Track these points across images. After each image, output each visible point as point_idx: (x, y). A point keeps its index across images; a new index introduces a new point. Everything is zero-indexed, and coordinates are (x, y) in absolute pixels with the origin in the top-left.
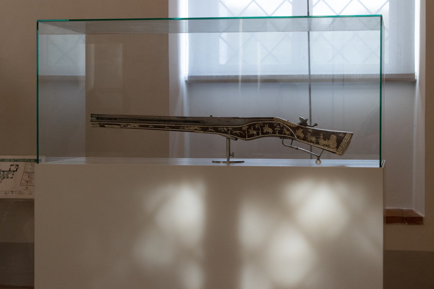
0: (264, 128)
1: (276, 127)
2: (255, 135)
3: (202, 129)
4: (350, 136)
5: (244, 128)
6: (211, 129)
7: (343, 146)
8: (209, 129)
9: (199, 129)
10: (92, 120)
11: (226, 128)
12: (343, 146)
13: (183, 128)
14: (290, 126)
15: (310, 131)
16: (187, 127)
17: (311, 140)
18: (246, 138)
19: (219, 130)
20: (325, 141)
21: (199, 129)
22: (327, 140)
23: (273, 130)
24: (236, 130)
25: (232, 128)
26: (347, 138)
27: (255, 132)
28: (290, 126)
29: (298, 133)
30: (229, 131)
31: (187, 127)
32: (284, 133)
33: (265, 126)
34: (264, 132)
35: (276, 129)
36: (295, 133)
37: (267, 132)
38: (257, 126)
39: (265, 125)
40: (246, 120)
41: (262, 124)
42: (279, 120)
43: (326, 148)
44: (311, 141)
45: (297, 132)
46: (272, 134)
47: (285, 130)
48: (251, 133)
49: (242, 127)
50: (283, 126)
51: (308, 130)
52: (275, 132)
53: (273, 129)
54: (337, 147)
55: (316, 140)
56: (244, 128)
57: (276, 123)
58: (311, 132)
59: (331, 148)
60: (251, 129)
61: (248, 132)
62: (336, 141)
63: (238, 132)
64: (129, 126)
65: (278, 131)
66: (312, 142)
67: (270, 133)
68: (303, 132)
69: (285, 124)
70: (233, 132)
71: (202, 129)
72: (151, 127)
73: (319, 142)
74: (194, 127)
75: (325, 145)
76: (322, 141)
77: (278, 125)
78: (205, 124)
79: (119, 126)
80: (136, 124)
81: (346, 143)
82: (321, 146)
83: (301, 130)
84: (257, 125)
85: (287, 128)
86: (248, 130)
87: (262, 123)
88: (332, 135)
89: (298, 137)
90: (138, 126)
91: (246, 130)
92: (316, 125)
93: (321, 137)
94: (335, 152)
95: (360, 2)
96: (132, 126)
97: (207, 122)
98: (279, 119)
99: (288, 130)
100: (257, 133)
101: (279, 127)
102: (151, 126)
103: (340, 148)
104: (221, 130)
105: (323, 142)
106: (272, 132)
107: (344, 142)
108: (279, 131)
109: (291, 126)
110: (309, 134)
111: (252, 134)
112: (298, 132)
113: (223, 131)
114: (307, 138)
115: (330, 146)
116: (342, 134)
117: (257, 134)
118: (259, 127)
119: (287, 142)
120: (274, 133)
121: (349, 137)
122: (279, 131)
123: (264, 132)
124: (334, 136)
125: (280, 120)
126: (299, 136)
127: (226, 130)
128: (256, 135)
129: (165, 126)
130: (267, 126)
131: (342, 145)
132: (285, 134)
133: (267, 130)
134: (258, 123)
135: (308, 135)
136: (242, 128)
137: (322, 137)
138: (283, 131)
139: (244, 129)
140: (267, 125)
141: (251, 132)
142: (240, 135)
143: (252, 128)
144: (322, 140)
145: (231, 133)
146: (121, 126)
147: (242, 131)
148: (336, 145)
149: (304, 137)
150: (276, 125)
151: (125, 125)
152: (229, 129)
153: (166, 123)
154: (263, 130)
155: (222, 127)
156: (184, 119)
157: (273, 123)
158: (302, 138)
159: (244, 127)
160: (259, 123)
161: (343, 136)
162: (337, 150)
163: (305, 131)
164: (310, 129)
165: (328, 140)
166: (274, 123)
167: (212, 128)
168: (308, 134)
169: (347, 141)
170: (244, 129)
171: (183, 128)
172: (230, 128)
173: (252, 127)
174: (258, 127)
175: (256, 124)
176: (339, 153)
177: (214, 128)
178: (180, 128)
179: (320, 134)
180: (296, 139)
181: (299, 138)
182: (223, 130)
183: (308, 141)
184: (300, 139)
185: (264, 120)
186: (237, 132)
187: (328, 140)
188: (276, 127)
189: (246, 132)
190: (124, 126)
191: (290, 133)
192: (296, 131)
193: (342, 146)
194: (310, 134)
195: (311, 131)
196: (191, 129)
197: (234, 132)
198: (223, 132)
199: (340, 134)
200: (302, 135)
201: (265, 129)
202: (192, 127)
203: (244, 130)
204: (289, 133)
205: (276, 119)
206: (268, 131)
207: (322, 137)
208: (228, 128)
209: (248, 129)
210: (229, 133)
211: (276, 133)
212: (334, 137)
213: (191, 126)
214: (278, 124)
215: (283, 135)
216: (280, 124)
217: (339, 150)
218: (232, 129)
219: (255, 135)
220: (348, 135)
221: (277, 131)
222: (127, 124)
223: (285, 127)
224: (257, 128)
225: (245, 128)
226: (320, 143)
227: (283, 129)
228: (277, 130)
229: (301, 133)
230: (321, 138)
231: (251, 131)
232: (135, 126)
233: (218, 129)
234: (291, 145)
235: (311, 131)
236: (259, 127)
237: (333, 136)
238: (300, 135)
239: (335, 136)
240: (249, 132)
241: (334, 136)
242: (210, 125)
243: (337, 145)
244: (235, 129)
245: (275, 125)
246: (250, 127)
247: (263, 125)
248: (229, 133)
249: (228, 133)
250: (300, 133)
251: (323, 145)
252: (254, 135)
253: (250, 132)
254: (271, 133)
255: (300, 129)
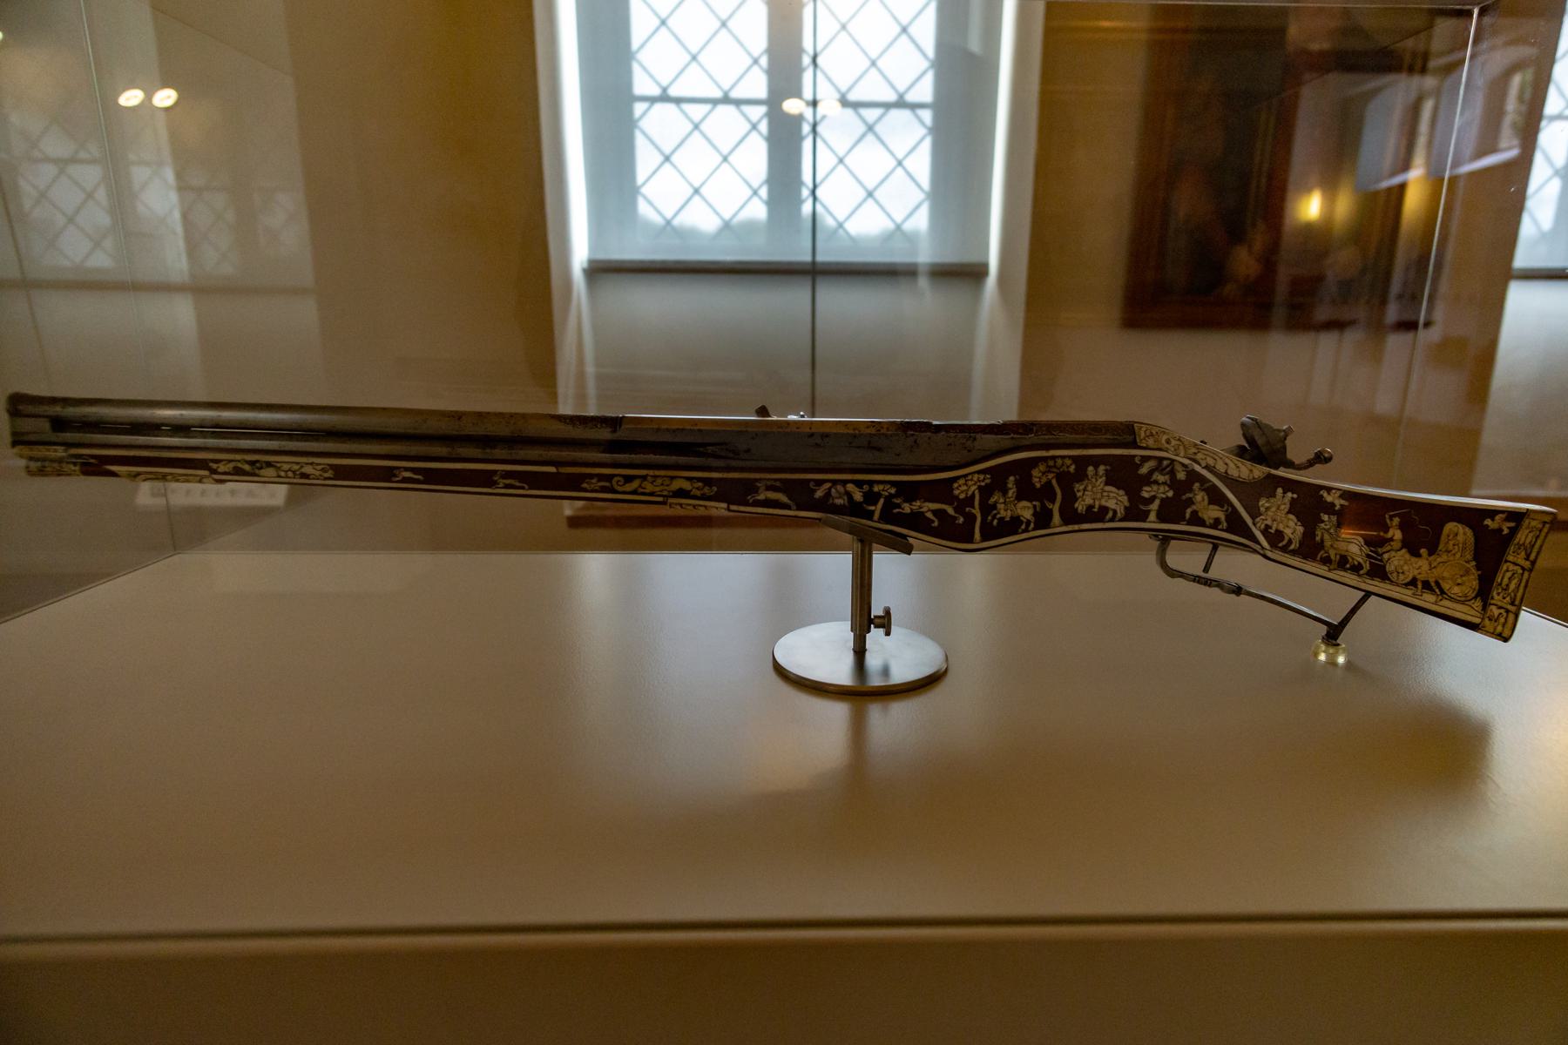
0: (1079, 487)
1: (1149, 483)
2: (1023, 527)
3: (715, 489)
4: (1547, 526)
5: (964, 488)
6: (768, 488)
7: (1512, 586)
8: (756, 491)
9: (698, 493)
10: (23, 434)
11: (859, 484)
12: (1512, 586)
13: (607, 484)
14: (1226, 473)
15: (1333, 505)
16: (629, 479)
17: (1343, 553)
18: (971, 541)
19: (819, 494)
20: (1414, 559)
21: (697, 488)
22: (1423, 551)
23: (1129, 500)
24: (915, 500)
25: (893, 483)
26: (1528, 541)
27: (1026, 511)
28: (1226, 473)
29: (1269, 513)
30: (875, 504)
31: (629, 479)
32: (1195, 513)
33: (1087, 476)
34: (1080, 506)
35: (1146, 495)
36: (1255, 514)
37: (1093, 507)
38: (1038, 477)
39: (1091, 468)
40: (975, 439)
41: (1068, 462)
42: (1168, 442)
43: (1428, 600)
44: (1343, 563)
45: (1262, 509)
46: (1121, 520)
47: (1200, 497)
48: (1003, 513)
49: (956, 479)
50: (1193, 476)
51: (1322, 496)
52: (1142, 507)
53: (1132, 491)
54: (1484, 594)
55: (1368, 556)
56: (964, 488)
57: (1155, 458)
58: (1337, 508)
59: (1451, 599)
60: (1005, 492)
61: (987, 509)
62: (1475, 558)
63: (928, 508)
64: (270, 472)
65: (1157, 502)
66: (1348, 566)
67: (1110, 514)
68: (1293, 509)
69: (1200, 465)
70: (898, 506)
71: (715, 489)
72: (405, 480)
73: (1384, 567)
74: (673, 478)
75: (1420, 586)
76: (1397, 560)
77: (1159, 468)
78: (734, 463)
79: (206, 473)
80: (312, 464)
81: (1523, 569)
82: (1398, 589)
83: (1284, 499)
84: (1042, 467)
85: (1214, 486)
86: (991, 495)
87: (1069, 457)
88: (1450, 527)
89: (1275, 538)
90: (326, 475)
91: (973, 494)
92: (1321, 458)
93: (1389, 535)
94: (1477, 621)
95: (707, 4)
96: (286, 472)
97: (748, 451)
98: (1165, 437)
99: (1216, 498)
100: (1035, 514)
101: (1164, 483)
102: (408, 474)
103: (1497, 597)
104: (828, 494)
105: (1405, 563)
106: (1126, 508)
107: (1515, 560)
108: (1162, 500)
109: (1229, 472)
110: (1325, 517)
111: (1008, 519)
112: (1267, 509)
113: (839, 502)
114: (1321, 545)
115: (1446, 586)
116: (1503, 516)
117: (1035, 523)
118: (1054, 482)
119: (1187, 557)
120: (1135, 512)
121: (1538, 537)
122: (1162, 500)
123: (1080, 508)
124: (1461, 531)
125: (1174, 442)
126: (1280, 534)
127: (858, 496)
128: (1032, 525)
129: (495, 472)
130: (1096, 474)
131: (1506, 580)
132: (1196, 520)
133: (1094, 499)
134: (1045, 459)
135: (1323, 525)
136: (956, 485)
137: (1395, 538)
138: (1190, 502)
139: (960, 491)
140: (1102, 468)
141: (1006, 510)
142: (936, 524)
143: (1010, 485)
144: (1400, 553)
145: (886, 516)
146: (214, 472)
147: (950, 504)
148: (1472, 582)
149: (1304, 534)
150: (1151, 472)
151: (239, 465)
152: (876, 489)
153: (499, 453)
154: (1076, 499)
155: (835, 482)
156: (604, 434)
157: (1135, 456)
158: (1292, 547)
159: (962, 481)
160: (1054, 458)
161: (1506, 531)
162: (1484, 608)
163: (1309, 504)
164: (1329, 489)
165: (1430, 554)
166: (1137, 460)
167: (778, 484)
168: (1323, 522)
169: (1527, 559)
170: (960, 491)
171: (607, 484)
172: (883, 483)
173: (1012, 478)
174: (1049, 482)
175: (1034, 462)
176: (1499, 629)
177: (786, 487)
178: (585, 485)
179: (1388, 521)
180: (1257, 547)
181: (1280, 545)
182: (840, 497)
183: (1326, 561)
184: (1284, 549)
185: (1079, 438)
186: (924, 509)
187: (1430, 554)
188: (1147, 480)
189: (973, 508)
190: (238, 472)
191: (1227, 517)
192: (1261, 503)
193: (1507, 585)
194: (1334, 518)
195: (1339, 503)
196: (649, 488)
197: (907, 508)
198: (838, 510)
199: (1493, 520)
200: (1291, 524)
201: (1085, 490)
202: (656, 477)
203: (962, 496)
204: (1223, 517)
205: (1152, 435)
206: (1103, 503)
207: (1398, 535)
208: (871, 483)
209: (986, 492)
210: (873, 512)
211: (1149, 512)
212: (1460, 538)
213: (651, 472)
214: (1165, 463)
215: (1188, 524)
216: (1173, 461)
217: (1496, 612)
218: (893, 491)
219: (1023, 527)
220: (1534, 523)
221: (1155, 506)
222: (252, 463)
223: (1201, 486)
224: (1038, 485)
225: (968, 484)
226: (1393, 568)
227: (1191, 495)
228: (1153, 499)
229: (1288, 513)
230: (1391, 539)
231: (1004, 503)
232: (308, 470)
233: (815, 491)
234: (1206, 570)
235: (1339, 503)
236: (1054, 482)
237: (1455, 530)
238: (1281, 527)
239: (1467, 529)
240: (994, 507)
241: (1461, 531)
242: (762, 464)
243: (1481, 578)
244: (910, 492)
245: (1144, 470)
246: (997, 480)
247: (1075, 469)
248: (876, 516)
249: (869, 516)
250: (1278, 513)
251: (1407, 585)
252: (1022, 522)
253: (999, 506)
254: (1119, 515)
255: (1280, 491)
